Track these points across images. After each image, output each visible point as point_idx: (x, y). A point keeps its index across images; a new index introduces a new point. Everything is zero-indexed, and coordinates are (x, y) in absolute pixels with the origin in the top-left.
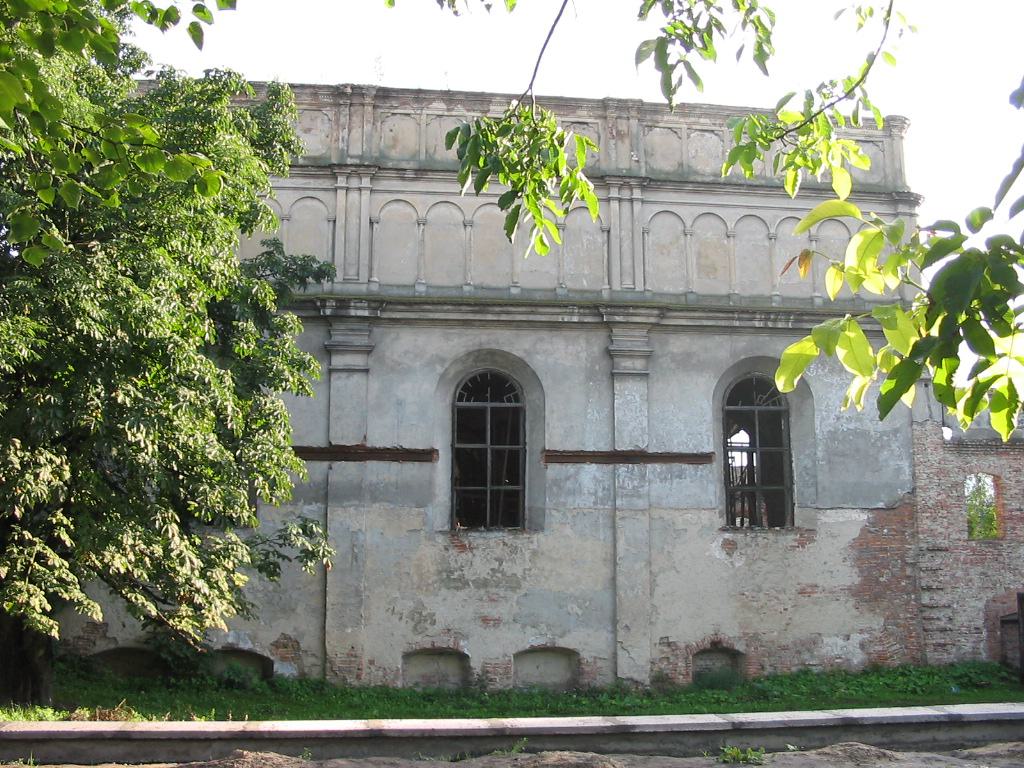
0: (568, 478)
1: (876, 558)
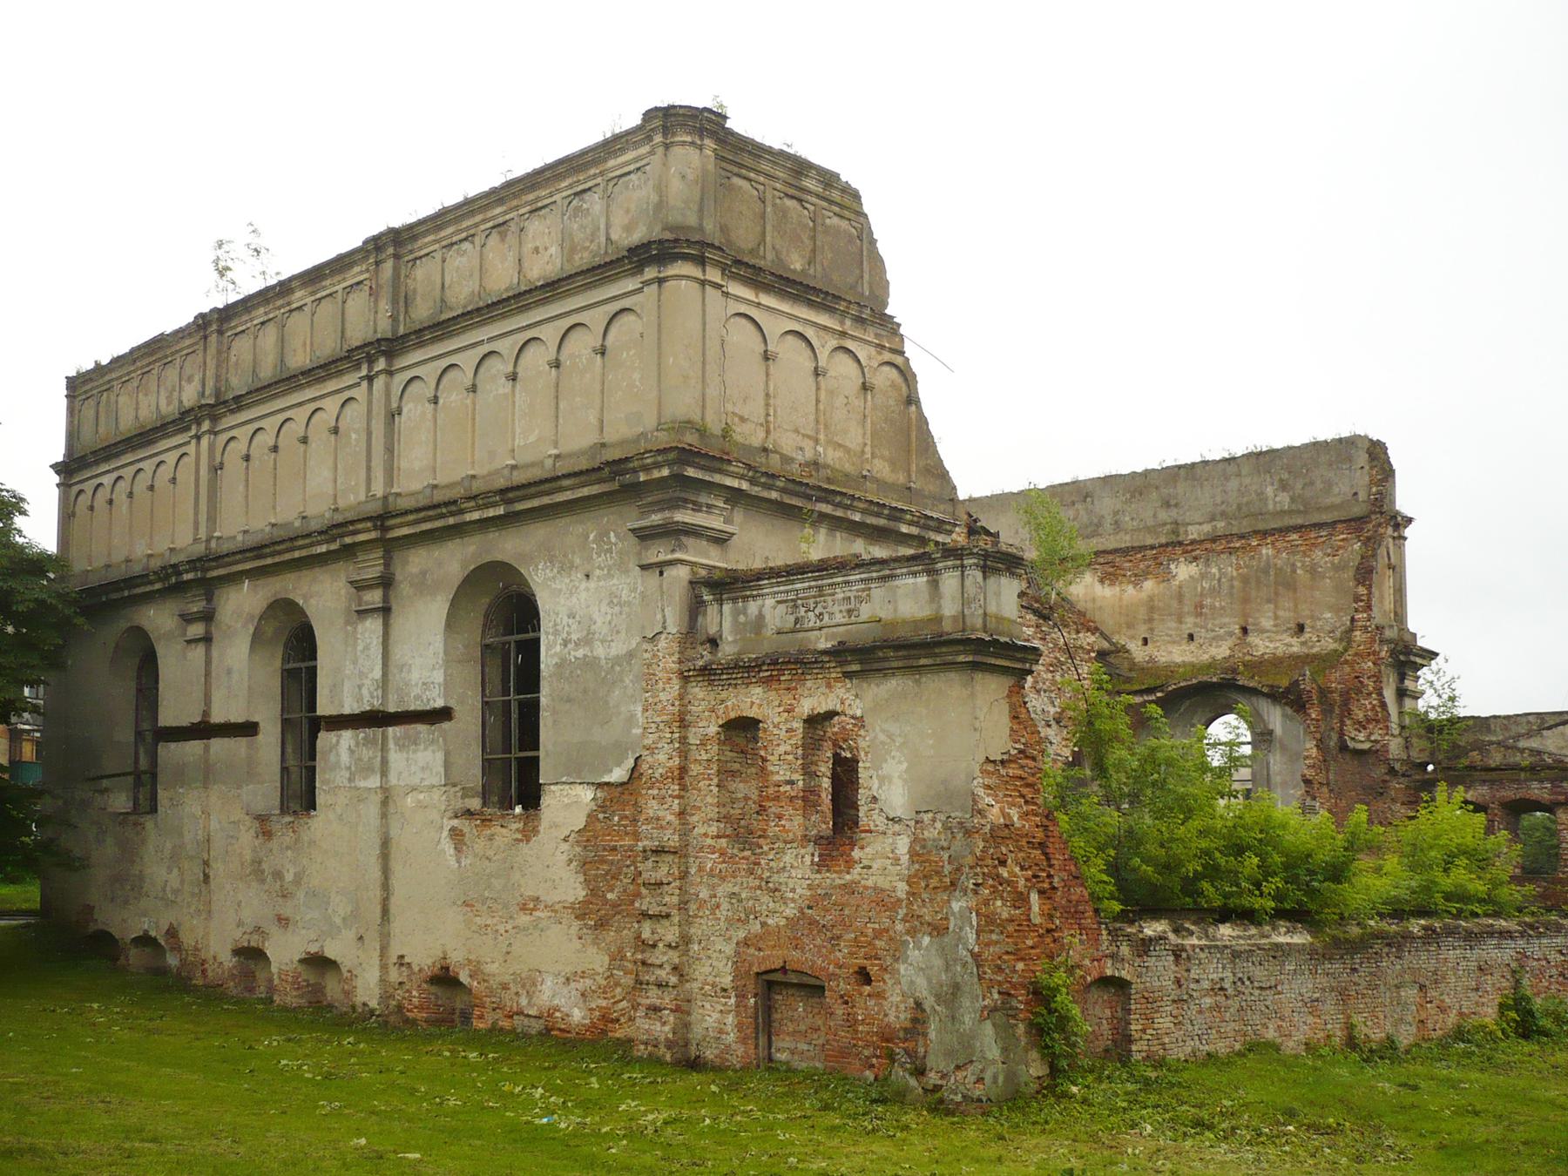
1: (603, 861)
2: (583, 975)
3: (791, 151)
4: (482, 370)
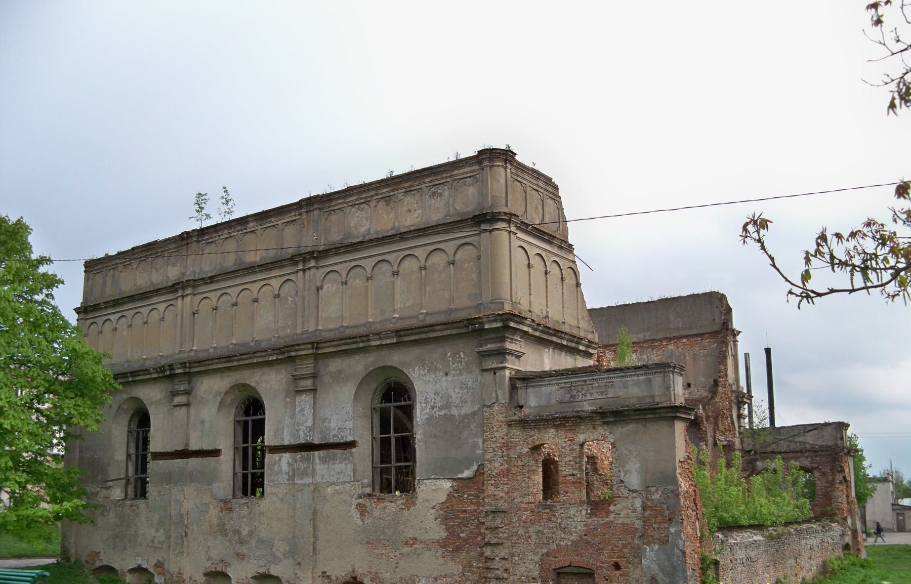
0: (275, 464)
3: (536, 168)
4: (376, 269)
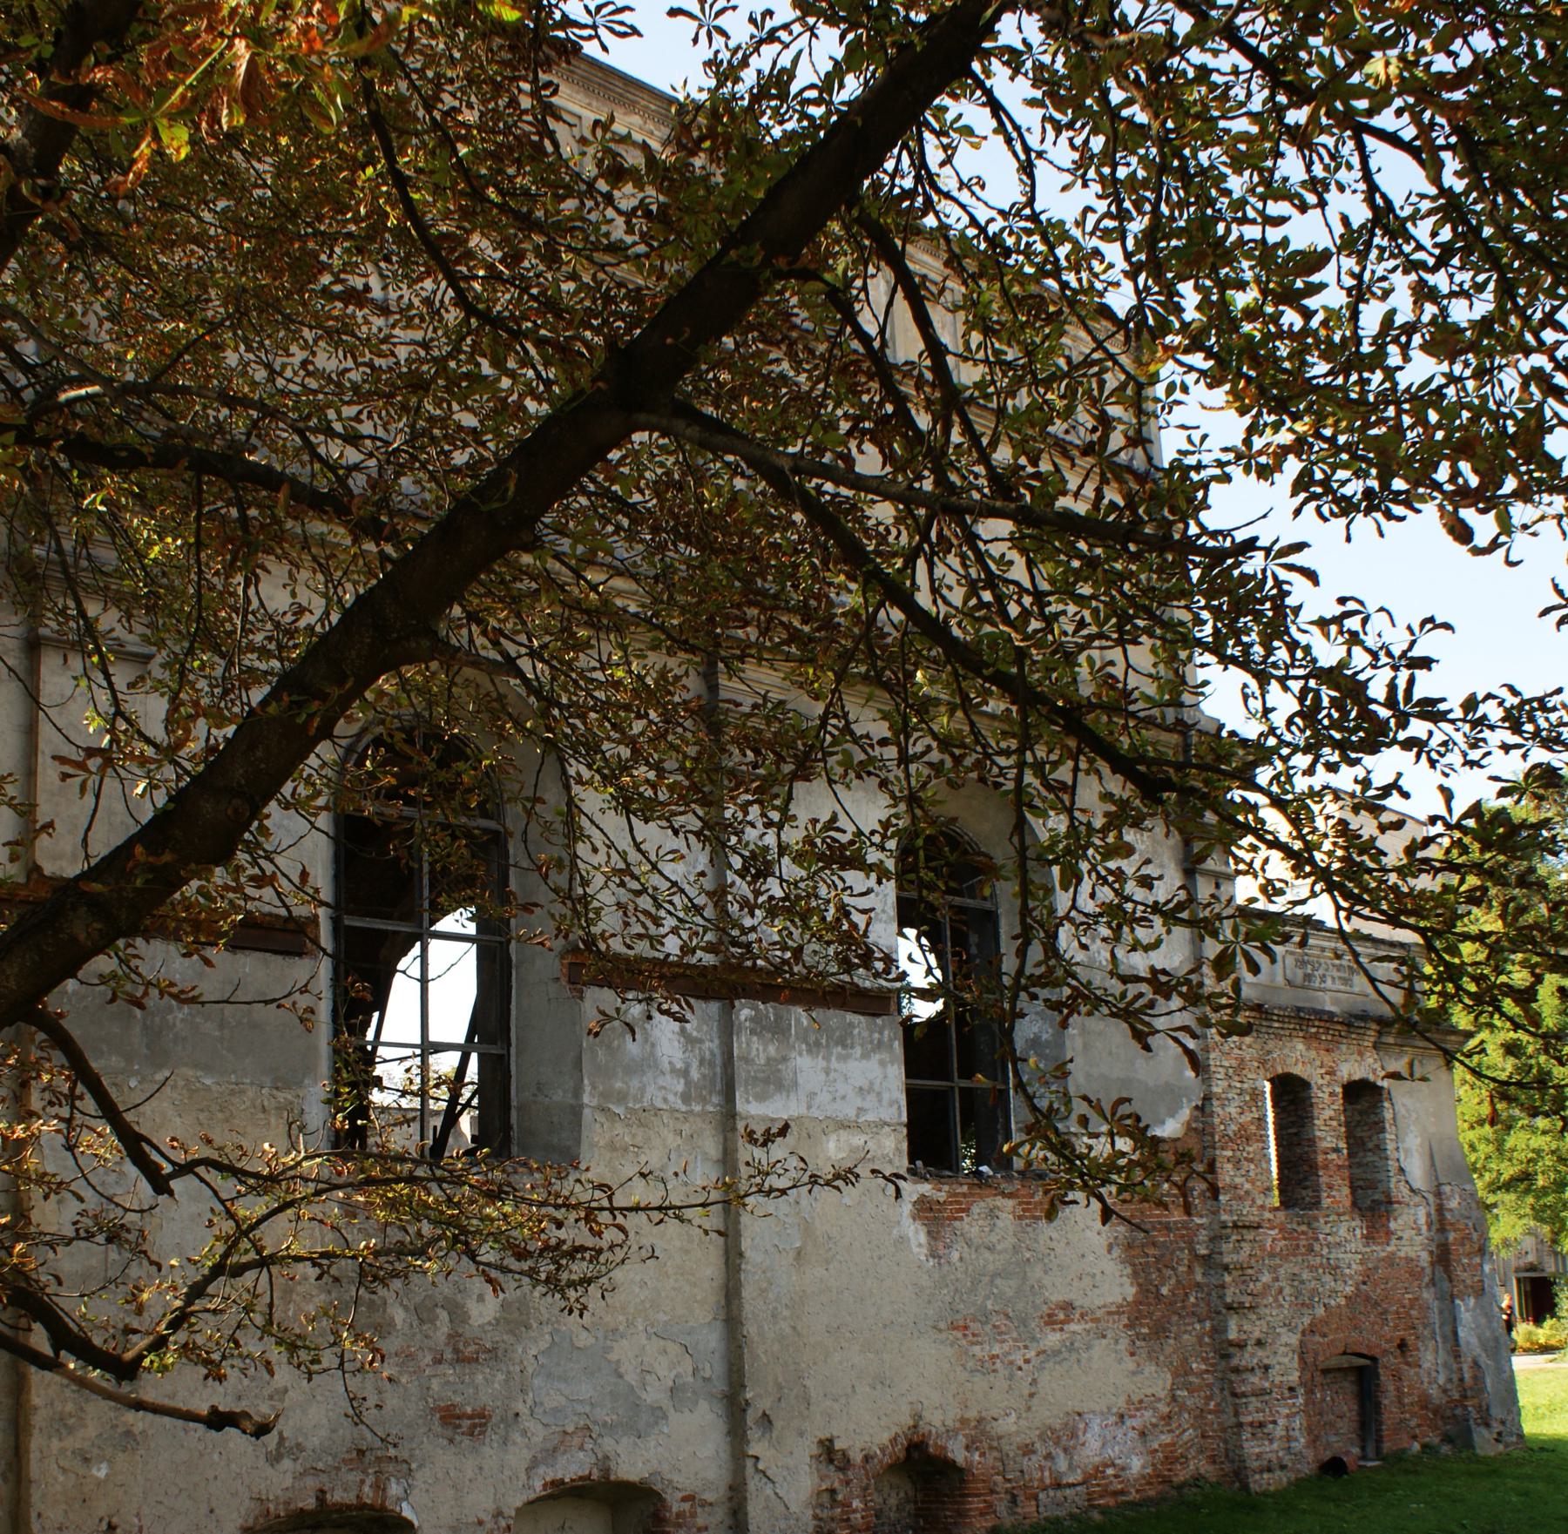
2: (1141, 1405)
